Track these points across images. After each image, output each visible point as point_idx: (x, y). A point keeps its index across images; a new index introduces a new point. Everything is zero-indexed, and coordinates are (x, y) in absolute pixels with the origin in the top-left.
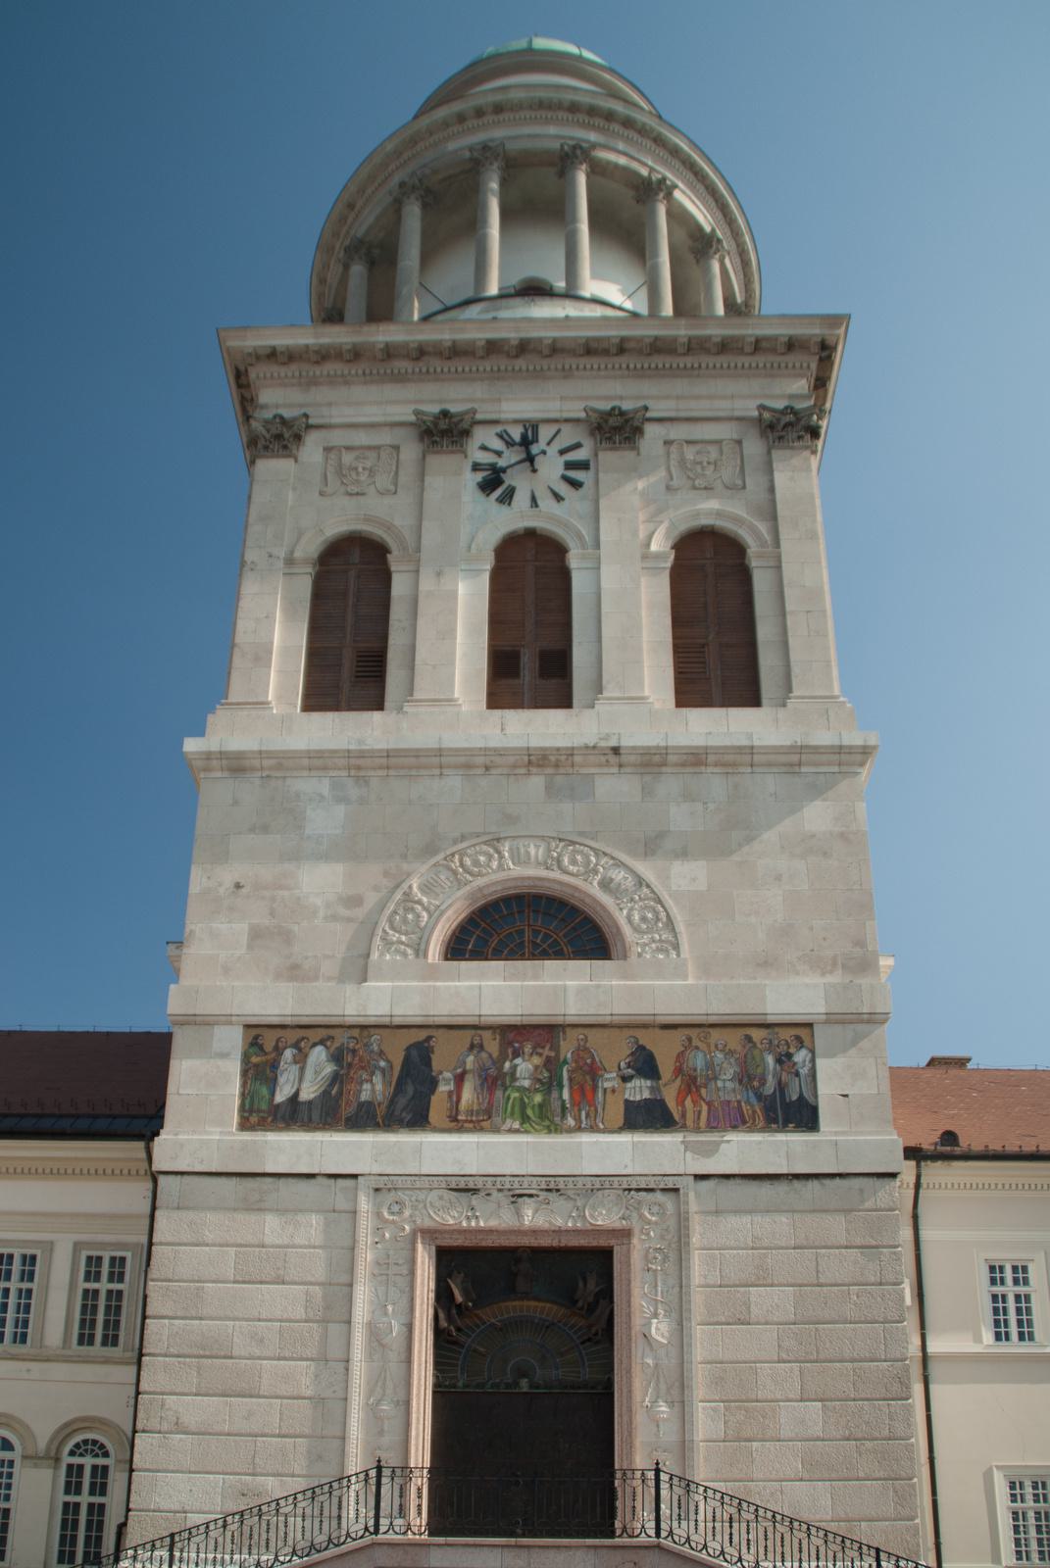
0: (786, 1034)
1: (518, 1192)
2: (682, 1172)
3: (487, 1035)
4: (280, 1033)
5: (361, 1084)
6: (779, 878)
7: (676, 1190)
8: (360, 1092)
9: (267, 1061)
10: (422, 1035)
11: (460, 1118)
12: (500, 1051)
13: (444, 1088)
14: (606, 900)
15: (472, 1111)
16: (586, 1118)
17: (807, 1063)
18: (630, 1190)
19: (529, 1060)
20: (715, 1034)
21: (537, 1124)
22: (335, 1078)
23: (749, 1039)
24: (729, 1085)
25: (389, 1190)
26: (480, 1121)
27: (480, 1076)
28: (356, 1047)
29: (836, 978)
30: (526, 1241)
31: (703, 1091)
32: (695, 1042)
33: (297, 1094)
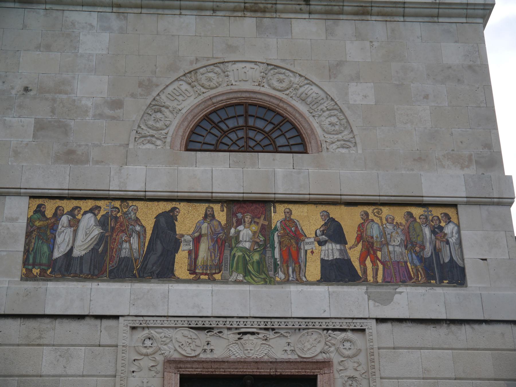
0: (437, 212)
2: (367, 317)
3: (217, 207)
4: (59, 203)
5: (121, 244)
6: (426, 97)
7: (363, 330)
8: (121, 249)
9: (48, 224)
10: (167, 206)
11: (197, 271)
12: (227, 220)
15: (207, 266)
16: (293, 272)
17: (454, 234)
18: (328, 330)
19: (249, 227)
20: (386, 211)
21: (256, 277)
22: (101, 238)
23: (410, 214)
24: (398, 249)
25: (143, 328)
27: (212, 239)
28: (118, 215)
29: (472, 171)
31: (379, 254)
32: (371, 216)
33: (71, 250)
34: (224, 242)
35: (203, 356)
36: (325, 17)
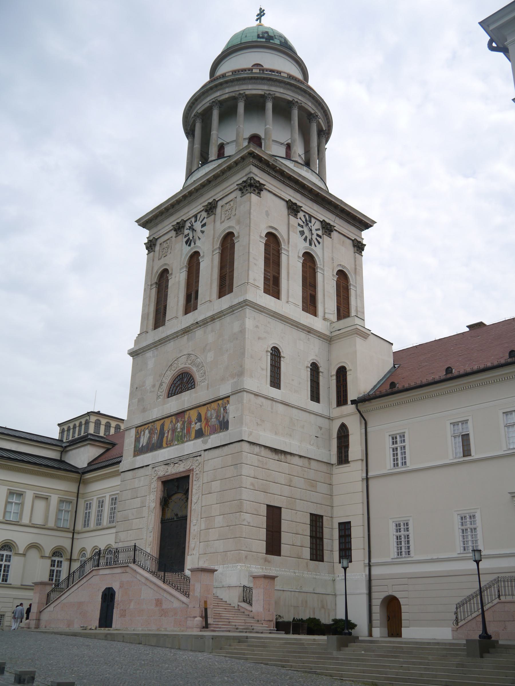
1: (175, 462)
13: (166, 435)
14: (195, 369)
20: (212, 404)
24: (214, 420)
26: (181, 439)
30: (175, 477)
32: (209, 408)
34: (174, 430)
35: (166, 474)
36: (204, 326)
